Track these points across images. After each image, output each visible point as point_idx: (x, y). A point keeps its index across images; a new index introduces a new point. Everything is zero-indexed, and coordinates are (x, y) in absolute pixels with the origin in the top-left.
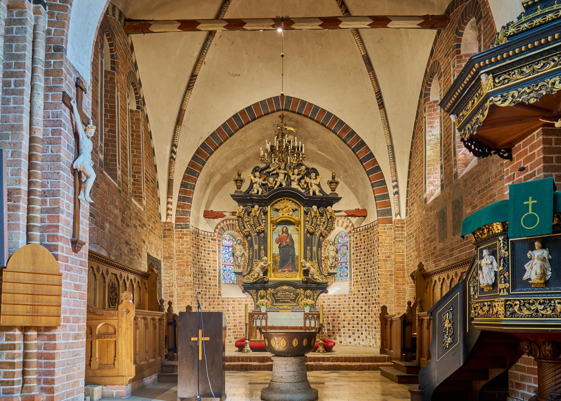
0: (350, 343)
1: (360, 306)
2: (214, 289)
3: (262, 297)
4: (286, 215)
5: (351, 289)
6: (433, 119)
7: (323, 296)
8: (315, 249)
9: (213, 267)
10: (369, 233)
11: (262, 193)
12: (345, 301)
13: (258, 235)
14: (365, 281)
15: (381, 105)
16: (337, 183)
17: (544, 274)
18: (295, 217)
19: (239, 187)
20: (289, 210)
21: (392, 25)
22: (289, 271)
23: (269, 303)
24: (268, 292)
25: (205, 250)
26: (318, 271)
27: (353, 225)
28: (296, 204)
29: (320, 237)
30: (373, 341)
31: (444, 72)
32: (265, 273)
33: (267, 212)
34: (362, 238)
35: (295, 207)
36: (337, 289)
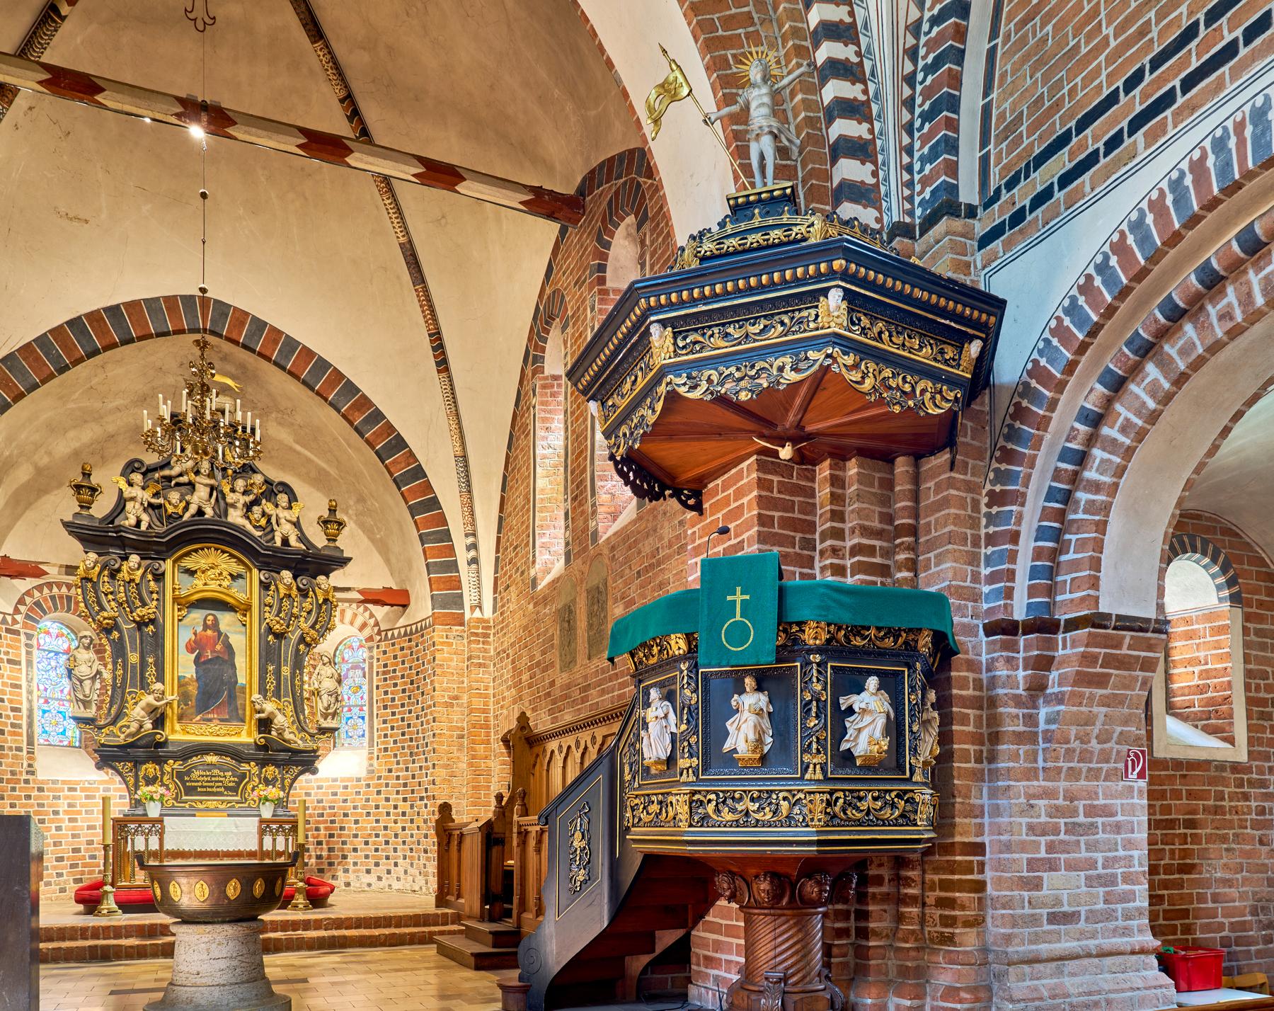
0: (369, 885)
1: (392, 803)
2: (15, 757)
3: (150, 781)
4: (213, 585)
5: (371, 765)
6: (550, 412)
7: (307, 781)
8: (286, 671)
9: (11, 701)
10: (413, 643)
11: (150, 526)
12: (358, 793)
13: (139, 629)
14: (403, 748)
15: (443, 364)
16: (341, 524)
17: (760, 741)
18: (238, 593)
19: (85, 506)
20: (220, 574)
21: (468, 188)
23: (169, 796)
24: (167, 768)
26: (293, 723)
27: (377, 624)
28: (240, 561)
29: (299, 644)
30: (420, 881)
31: (573, 316)
32: (159, 722)
33: (163, 574)
34: (399, 653)
35: (236, 568)
36: (343, 766)
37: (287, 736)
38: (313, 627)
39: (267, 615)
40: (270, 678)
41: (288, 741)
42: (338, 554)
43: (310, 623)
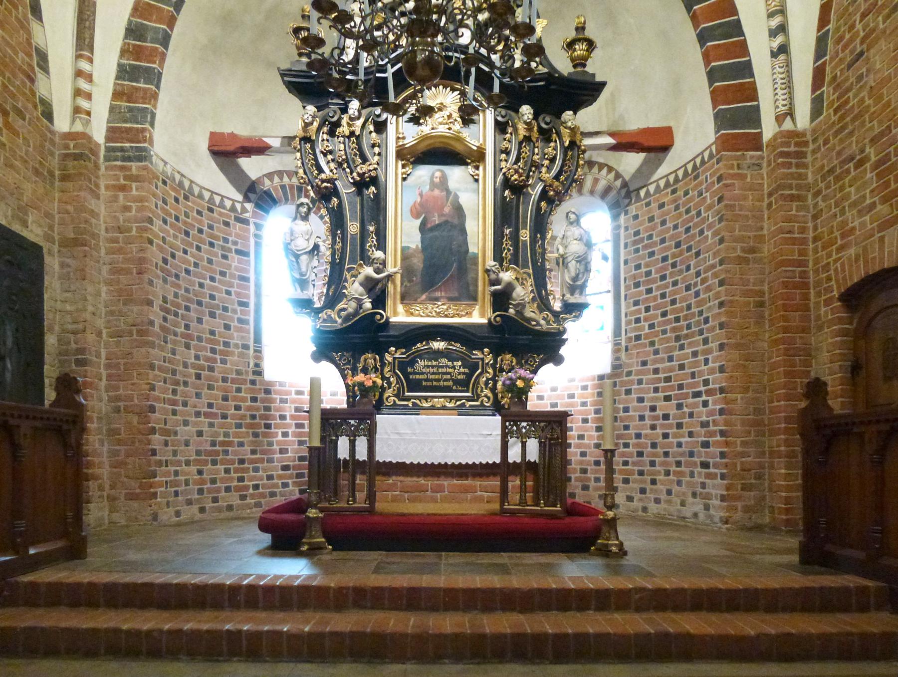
1: (647, 404)
4: (442, 130)
8: (525, 235)
20: (450, 117)
22: (451, 299)
25: (212, 245)
26: (534, 299)
32: (380, 301)
37: (528, 313)
38: (557, 178)
39: (503, 164)
40: (507, 244)
41: (528, 320)
42: (588, 79)
43: (554, 172)
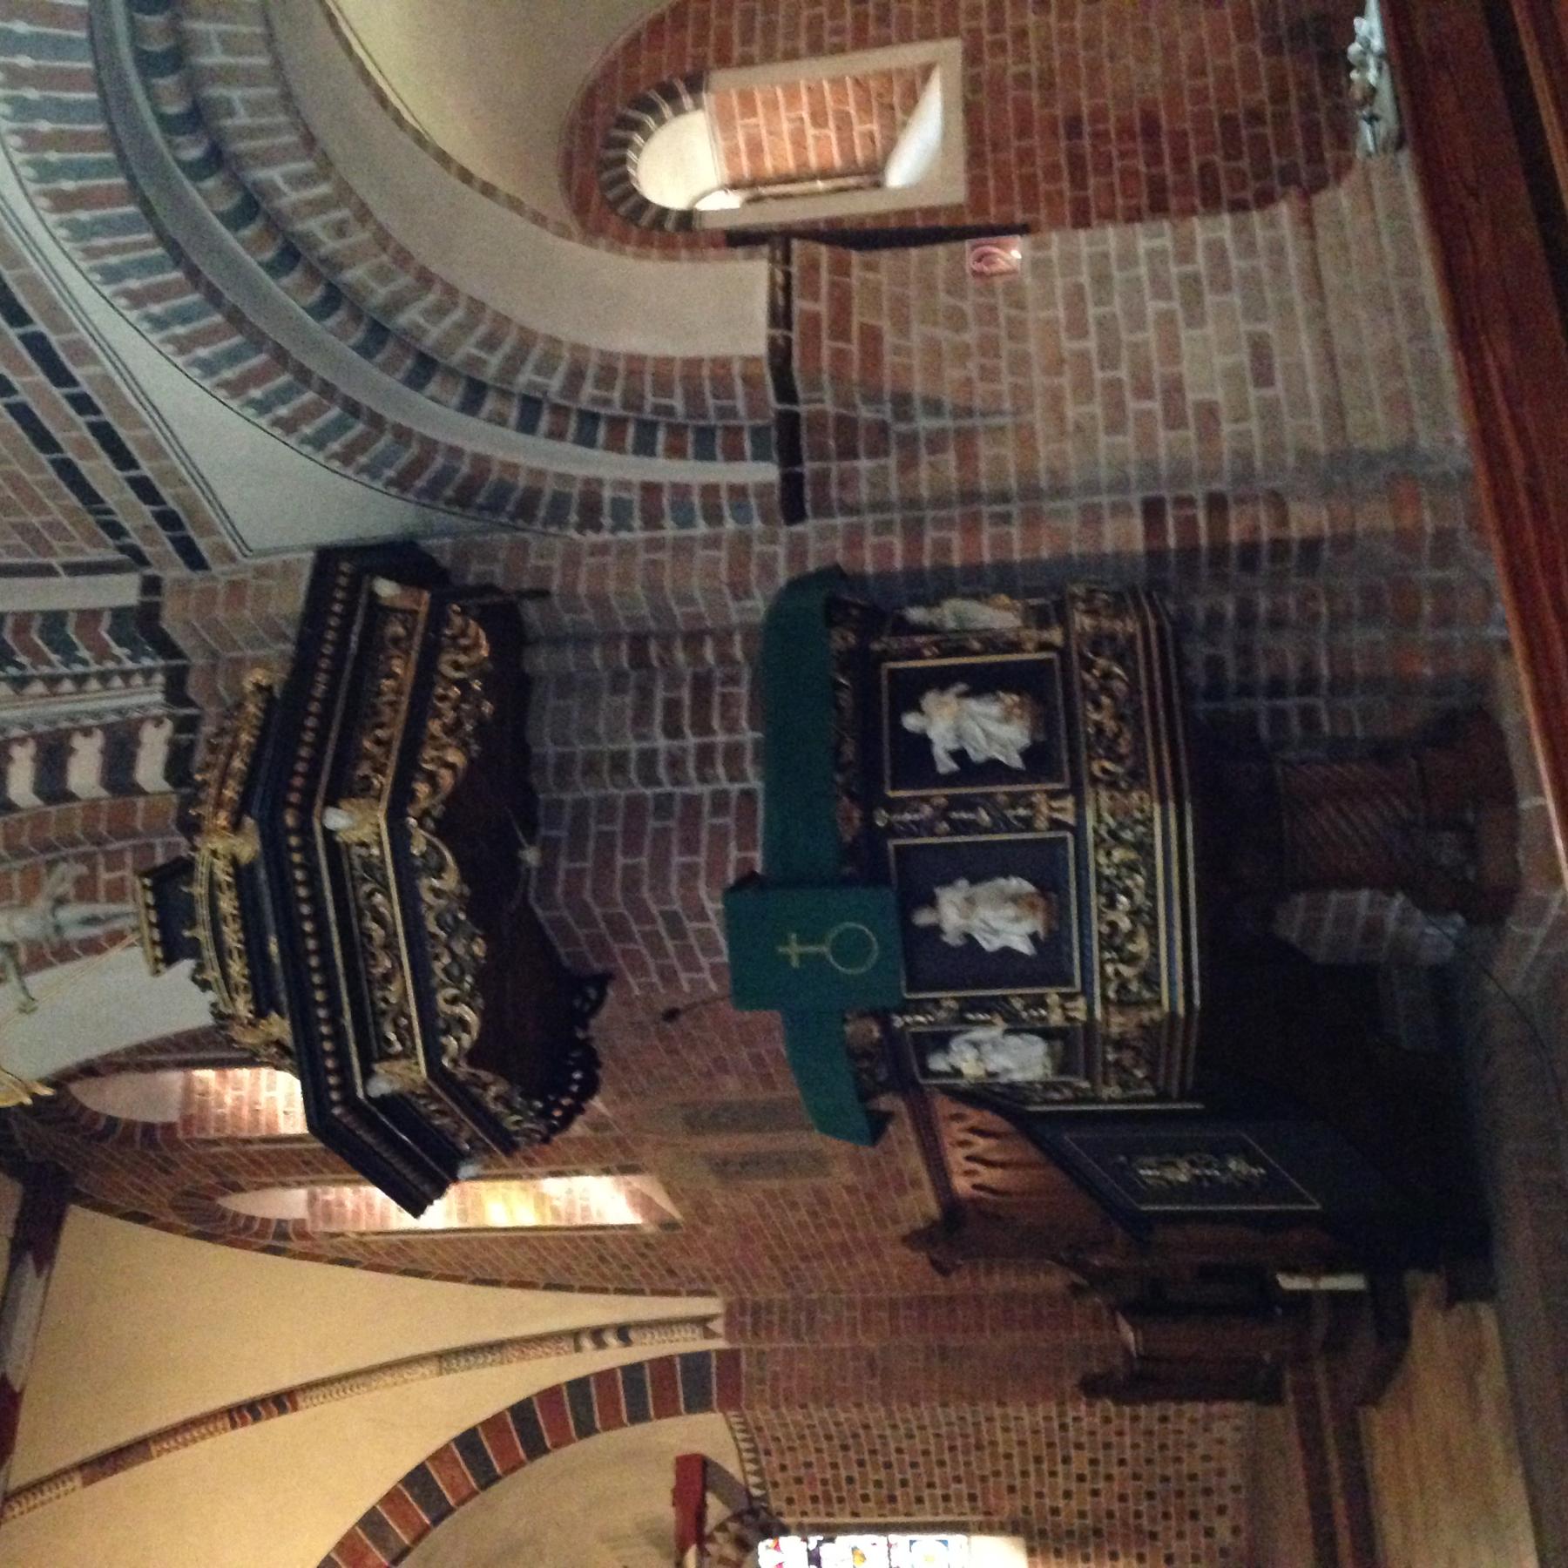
1: (1074, 1486)
